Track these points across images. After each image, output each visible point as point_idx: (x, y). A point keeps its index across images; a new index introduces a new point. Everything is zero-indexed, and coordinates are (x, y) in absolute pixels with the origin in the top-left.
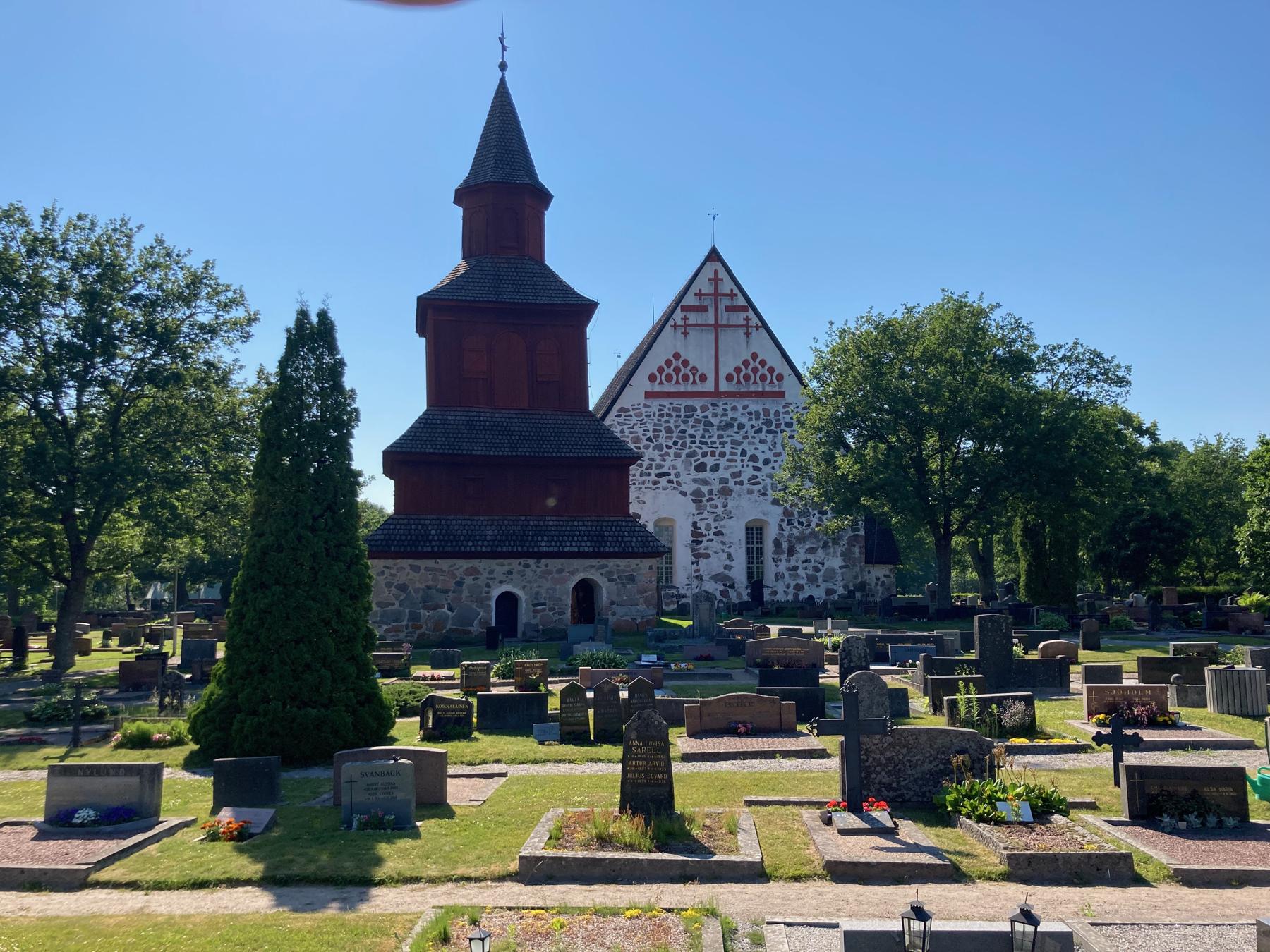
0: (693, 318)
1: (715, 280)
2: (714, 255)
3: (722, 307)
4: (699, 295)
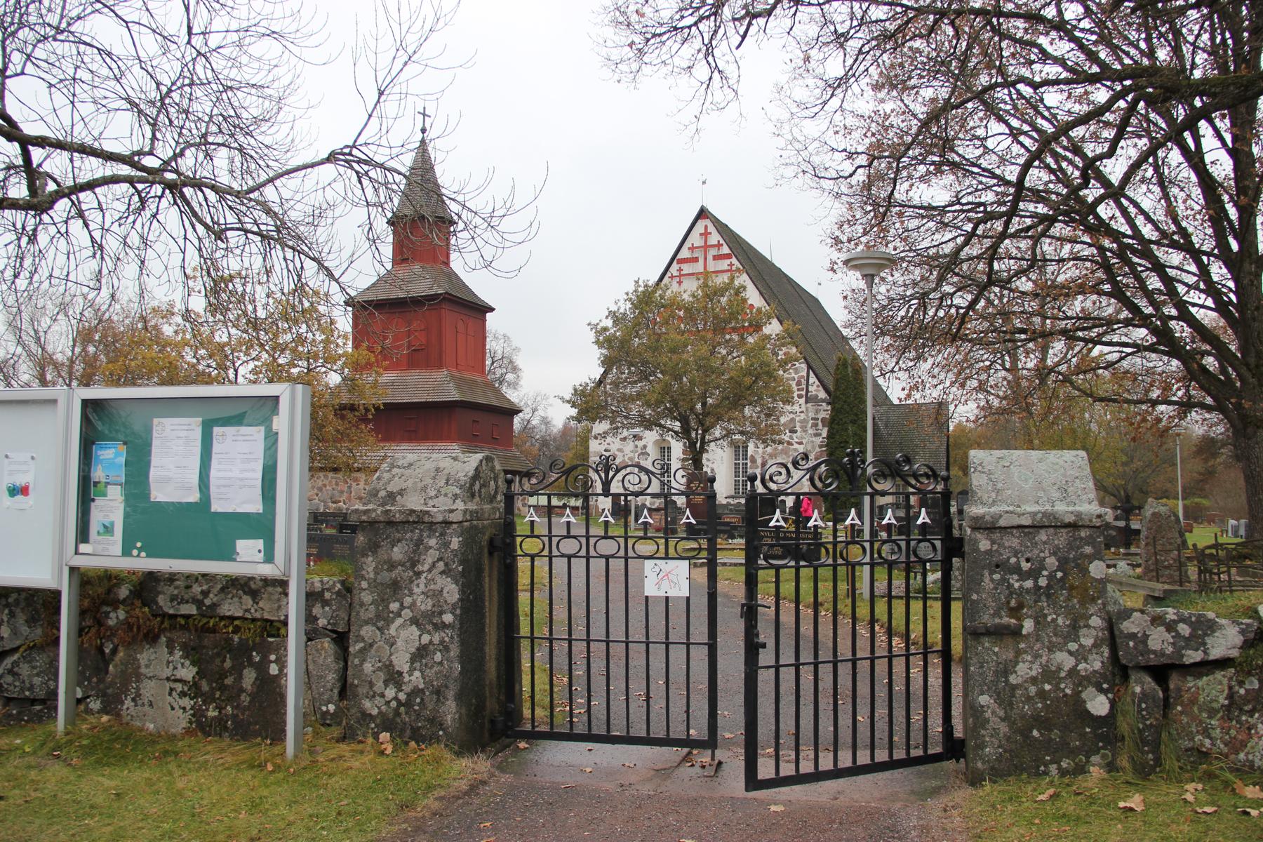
0: (687, 268)
1: (706, 234)
2: (703, 213)
3: (710, 258)
4: (692, 249)
